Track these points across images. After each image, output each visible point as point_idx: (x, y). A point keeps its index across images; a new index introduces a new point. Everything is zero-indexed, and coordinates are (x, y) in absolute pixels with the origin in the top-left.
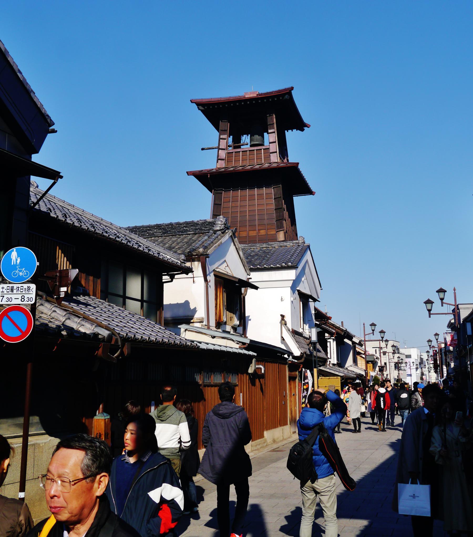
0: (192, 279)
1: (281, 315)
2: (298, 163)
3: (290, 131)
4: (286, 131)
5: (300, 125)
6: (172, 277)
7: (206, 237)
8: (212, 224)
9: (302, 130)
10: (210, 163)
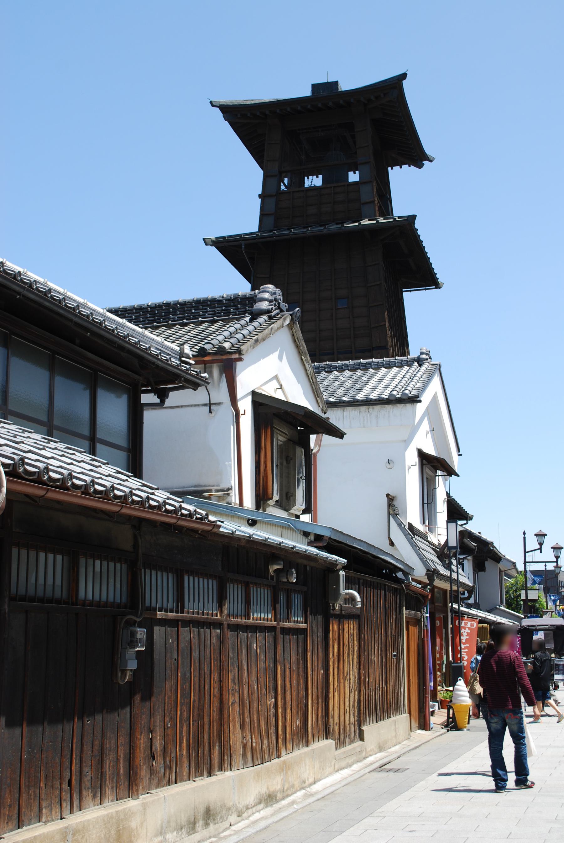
0: (208, 408)
1: (388, 495)
2: (414, 217)
3: (397, 168)
4: (389, 169)
5: (416, 156)
6: (163, 395)
7: (238, 326)
8: (250, 301)
9: (420, 166)
10: (245, 219)
